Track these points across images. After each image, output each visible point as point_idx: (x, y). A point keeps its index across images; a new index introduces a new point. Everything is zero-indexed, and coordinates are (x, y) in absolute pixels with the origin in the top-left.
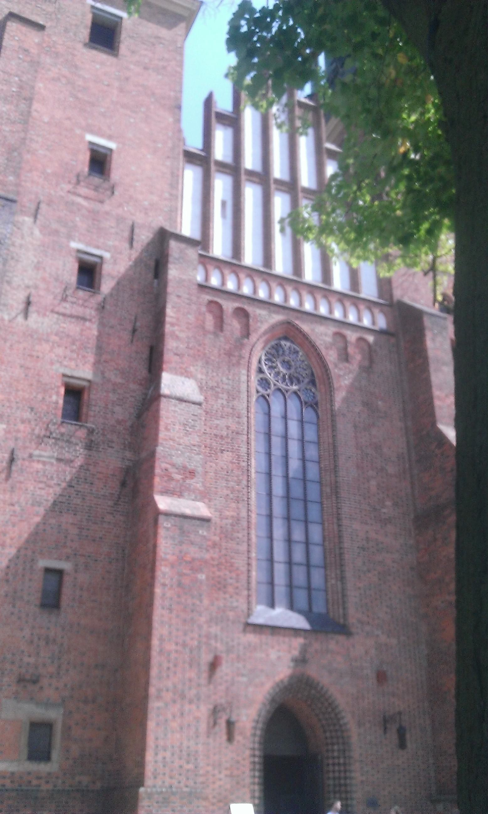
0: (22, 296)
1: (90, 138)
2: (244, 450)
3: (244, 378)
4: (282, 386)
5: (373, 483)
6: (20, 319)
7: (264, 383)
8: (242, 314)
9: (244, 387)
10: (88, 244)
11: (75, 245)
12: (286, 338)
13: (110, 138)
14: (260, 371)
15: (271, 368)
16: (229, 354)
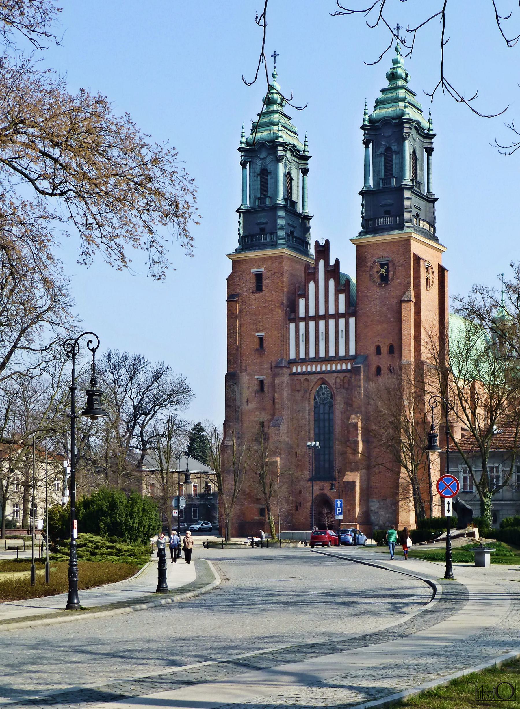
0: (246, 400)
1: (257, 334)
2: (307, 429)
3: (307, 406)
4: (322, 402)
5: (346, 431)
6: (247, 407)
7: (316, 403)
8: (306, 380)
9: (307, 408)
10: (259, 375)
11: (256, 377)
12: (323, 384)
13: (262, 331)
14: (315, 399)
15: (319, 396)
16: (303, 397)
